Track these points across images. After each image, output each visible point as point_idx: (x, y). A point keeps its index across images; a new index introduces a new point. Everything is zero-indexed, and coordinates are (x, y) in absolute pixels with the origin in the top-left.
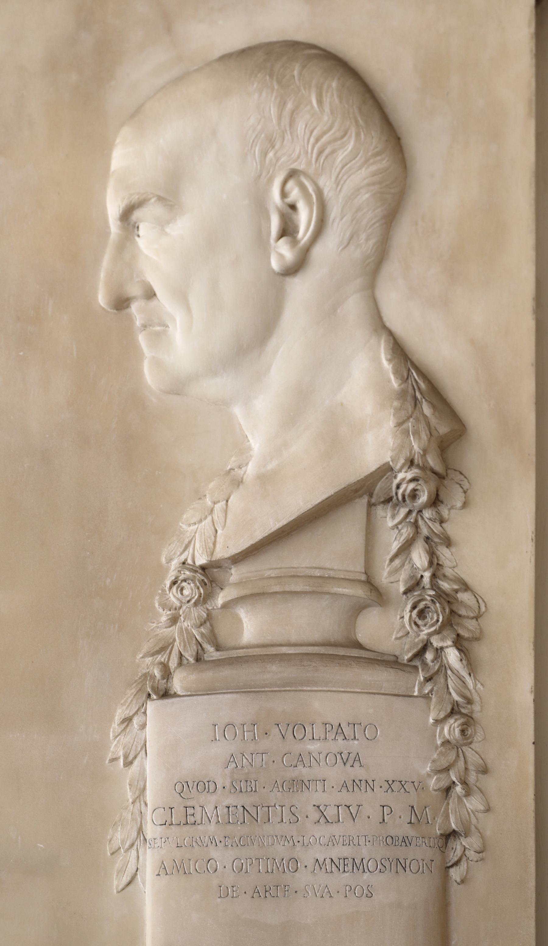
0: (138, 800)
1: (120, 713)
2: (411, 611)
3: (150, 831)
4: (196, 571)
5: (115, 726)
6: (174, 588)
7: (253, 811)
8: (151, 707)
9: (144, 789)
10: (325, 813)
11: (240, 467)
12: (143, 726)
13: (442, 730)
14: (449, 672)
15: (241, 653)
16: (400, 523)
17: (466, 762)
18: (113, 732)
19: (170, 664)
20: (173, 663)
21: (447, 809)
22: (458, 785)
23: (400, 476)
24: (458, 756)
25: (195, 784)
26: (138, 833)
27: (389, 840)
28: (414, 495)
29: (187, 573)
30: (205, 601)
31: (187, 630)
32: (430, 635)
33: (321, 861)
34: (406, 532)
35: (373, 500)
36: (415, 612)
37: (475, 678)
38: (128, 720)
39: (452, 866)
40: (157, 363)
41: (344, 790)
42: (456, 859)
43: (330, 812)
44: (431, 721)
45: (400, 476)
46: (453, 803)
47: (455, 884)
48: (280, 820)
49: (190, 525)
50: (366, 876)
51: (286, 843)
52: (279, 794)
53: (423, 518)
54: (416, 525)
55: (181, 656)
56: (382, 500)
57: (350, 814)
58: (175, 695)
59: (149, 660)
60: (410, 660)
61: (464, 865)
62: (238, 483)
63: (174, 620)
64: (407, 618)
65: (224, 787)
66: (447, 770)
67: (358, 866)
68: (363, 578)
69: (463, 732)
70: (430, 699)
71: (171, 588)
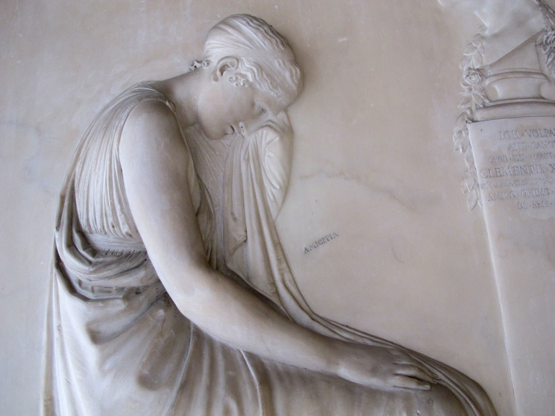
1: (456, 129)
6: (468, 78)
8: (470, 126)
12: (467, 134)
16: (548, 52)
18: (455, 138)
19: (472, 109)
20: (474, 108)
25: (498, 158)
31: (476, 94)
38: (460, 132)
48: (537, 172)
59: (463, 107)
63: (470, 90)
65: (510, 159)
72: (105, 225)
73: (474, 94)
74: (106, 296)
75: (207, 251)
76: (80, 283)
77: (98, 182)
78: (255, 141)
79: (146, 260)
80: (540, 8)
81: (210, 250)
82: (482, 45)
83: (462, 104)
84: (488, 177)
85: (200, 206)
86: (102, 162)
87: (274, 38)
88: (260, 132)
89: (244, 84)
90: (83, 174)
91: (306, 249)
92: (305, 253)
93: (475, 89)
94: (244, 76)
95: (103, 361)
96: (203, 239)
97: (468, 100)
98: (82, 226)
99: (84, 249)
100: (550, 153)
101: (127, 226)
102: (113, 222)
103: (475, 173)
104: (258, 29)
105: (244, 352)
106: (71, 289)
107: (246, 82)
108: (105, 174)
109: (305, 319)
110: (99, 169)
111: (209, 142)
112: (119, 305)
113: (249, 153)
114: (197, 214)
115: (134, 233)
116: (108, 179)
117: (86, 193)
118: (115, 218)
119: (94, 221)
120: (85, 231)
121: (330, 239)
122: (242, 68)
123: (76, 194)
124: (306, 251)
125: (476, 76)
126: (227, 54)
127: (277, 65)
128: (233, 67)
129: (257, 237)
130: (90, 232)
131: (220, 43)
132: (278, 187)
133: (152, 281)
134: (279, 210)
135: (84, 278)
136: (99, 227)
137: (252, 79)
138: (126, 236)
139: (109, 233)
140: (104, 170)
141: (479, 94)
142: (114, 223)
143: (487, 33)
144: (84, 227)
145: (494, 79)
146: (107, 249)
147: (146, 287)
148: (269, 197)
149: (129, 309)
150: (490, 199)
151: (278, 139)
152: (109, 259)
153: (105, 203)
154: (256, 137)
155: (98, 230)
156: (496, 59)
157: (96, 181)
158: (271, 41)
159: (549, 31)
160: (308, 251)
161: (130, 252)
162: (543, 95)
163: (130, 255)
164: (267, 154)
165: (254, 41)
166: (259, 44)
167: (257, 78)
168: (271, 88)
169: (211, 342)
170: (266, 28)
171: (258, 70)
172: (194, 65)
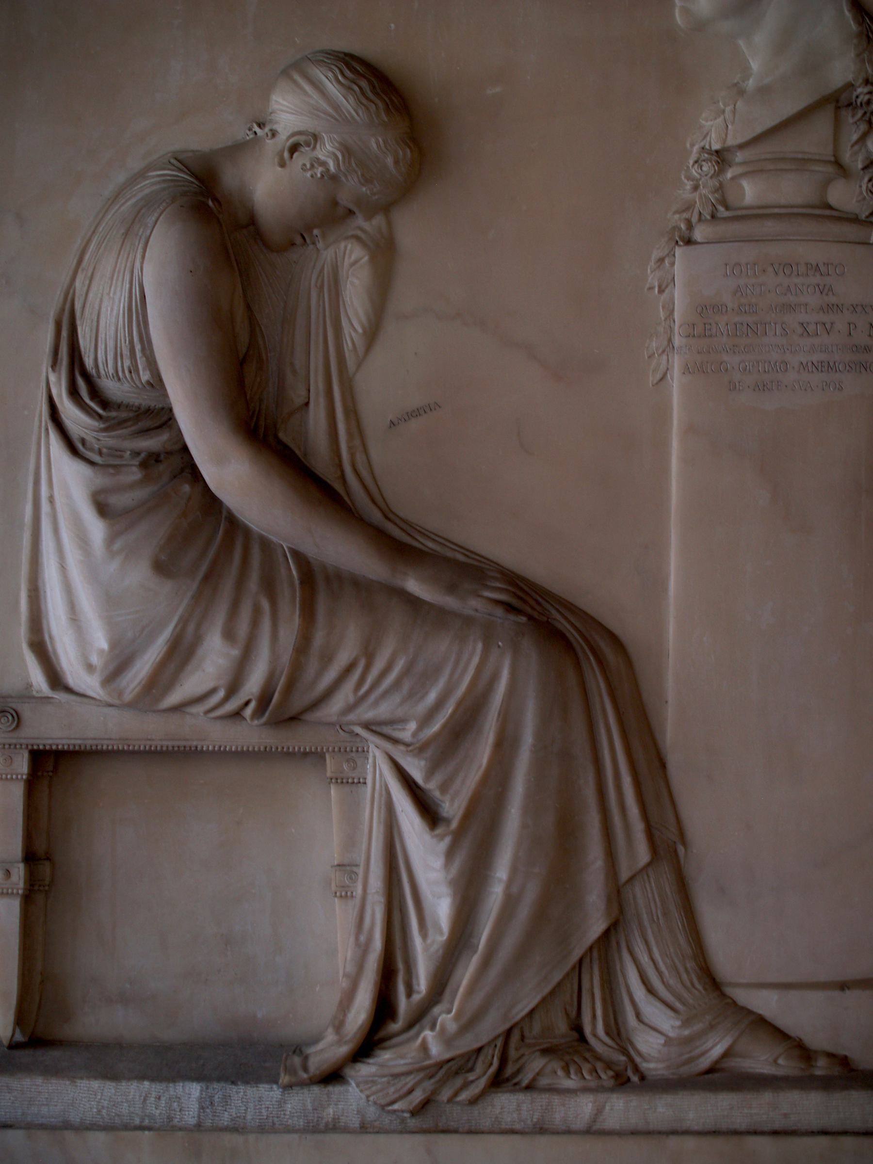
0: (668, 320)
1: (656, 255)
2: (868, 183)
3: (677, 341)
4: (712, 154)
5: (652, 263)
6: (696, 166)
8: (678, 251)
9: (673, 310)
11: (743, 82)
12: (673, 264)
15: (744, 212)
16: (858, 120)
18: (650, 269)
20: (694, 219)
26: (669, 344)
27: (854, 349)
29: (706, 155)
30: (718, 175)
31: (705, 195)
38: (661, 260)
40: (685, 11)
43: (811, 328)
45: (859, 90)
49: (707, 121)
51: (779, 350)
57: (825, 330)
58: (696, 243)
59: (677, 216)
60: (867, 217)
62: (741, 92)
63: (696, 188)
64: (864, 188)
67: (832, 367)
68: (832, 159)
71: (693, 165)
72: (120, 369)
74: (117, 462)
75: (254, 412)
76: (83, 442)
77: (112, 309)
78: (334, 259)
79: (170, 419)
80: (855, 41)
81: (257, 412)
83: (676, 212)
84: (689, 336)
85: (248, 351)
86: (119, 284)
87: (373, 103)
88: (342, 245)
89: (322, 176)
90: (91, 295)
91: (392, 423)
92: (390, 426)
93: (703, 187)
94: (323, 164)
95: (111, 540)
96: (248, 397)
97: (689, 207)
98: (87, 367)
99: (92, 399)
100: (806, 305)
101: (148, 372)
102: (131, 365)
103: (671, 329)
104: (350, 88)
105: (290, 549)
106: (72, 447)
107: (325, 174)
108: (122, 300)
109: (376, 516)
110: (115, 293)
111: (267, 255)
112: (134, 474)
113: (323, 276)
114: (242, 362)
115: (157, 383)
116: (126, 309)
117: (95, 324)
118: (133, 360)
119: (105, 362)
120: (90, 374)
121: (428, 410)
122: (322, 150)
123: (78, 322)
124: (392, 425)
126: (302, 127)
127: (374, 146)
128: (309, 146)
129: (322, 401)
130: (97, 376)
131: (293, 107)
132: (360, 330)
133: (177, 447)
134: (359, 365)
135: (90, 437)
136: (111, 370)
137: (335, 169)
138: (146, 386)
139: (124, 380)
140: (121, 295)
142: (132, 368)
143: (751, 84)
144: (91, 369)
146: (119, 401)
147: (169, 453)
148: (347, 343)
149: (146, 480)
150: (686, 370)
151: (366, 258)
152: (124, 415)
153: (121, 340)
154: (336, 253)
155: (109, 374)
156: (749, 136)
157: (109, 309)
158: (368, 109)
159: (859, 87)
160: (394, 425)
161: (149, 407)
163: (150, 411)
164: (350, 279)
165: (342, 108)
166: (350, 113)
167: (342, 168)
168: (362, 181)
169: (247, 532)
170: (364, 84)
171: (343, 156)
172: (254, 130)
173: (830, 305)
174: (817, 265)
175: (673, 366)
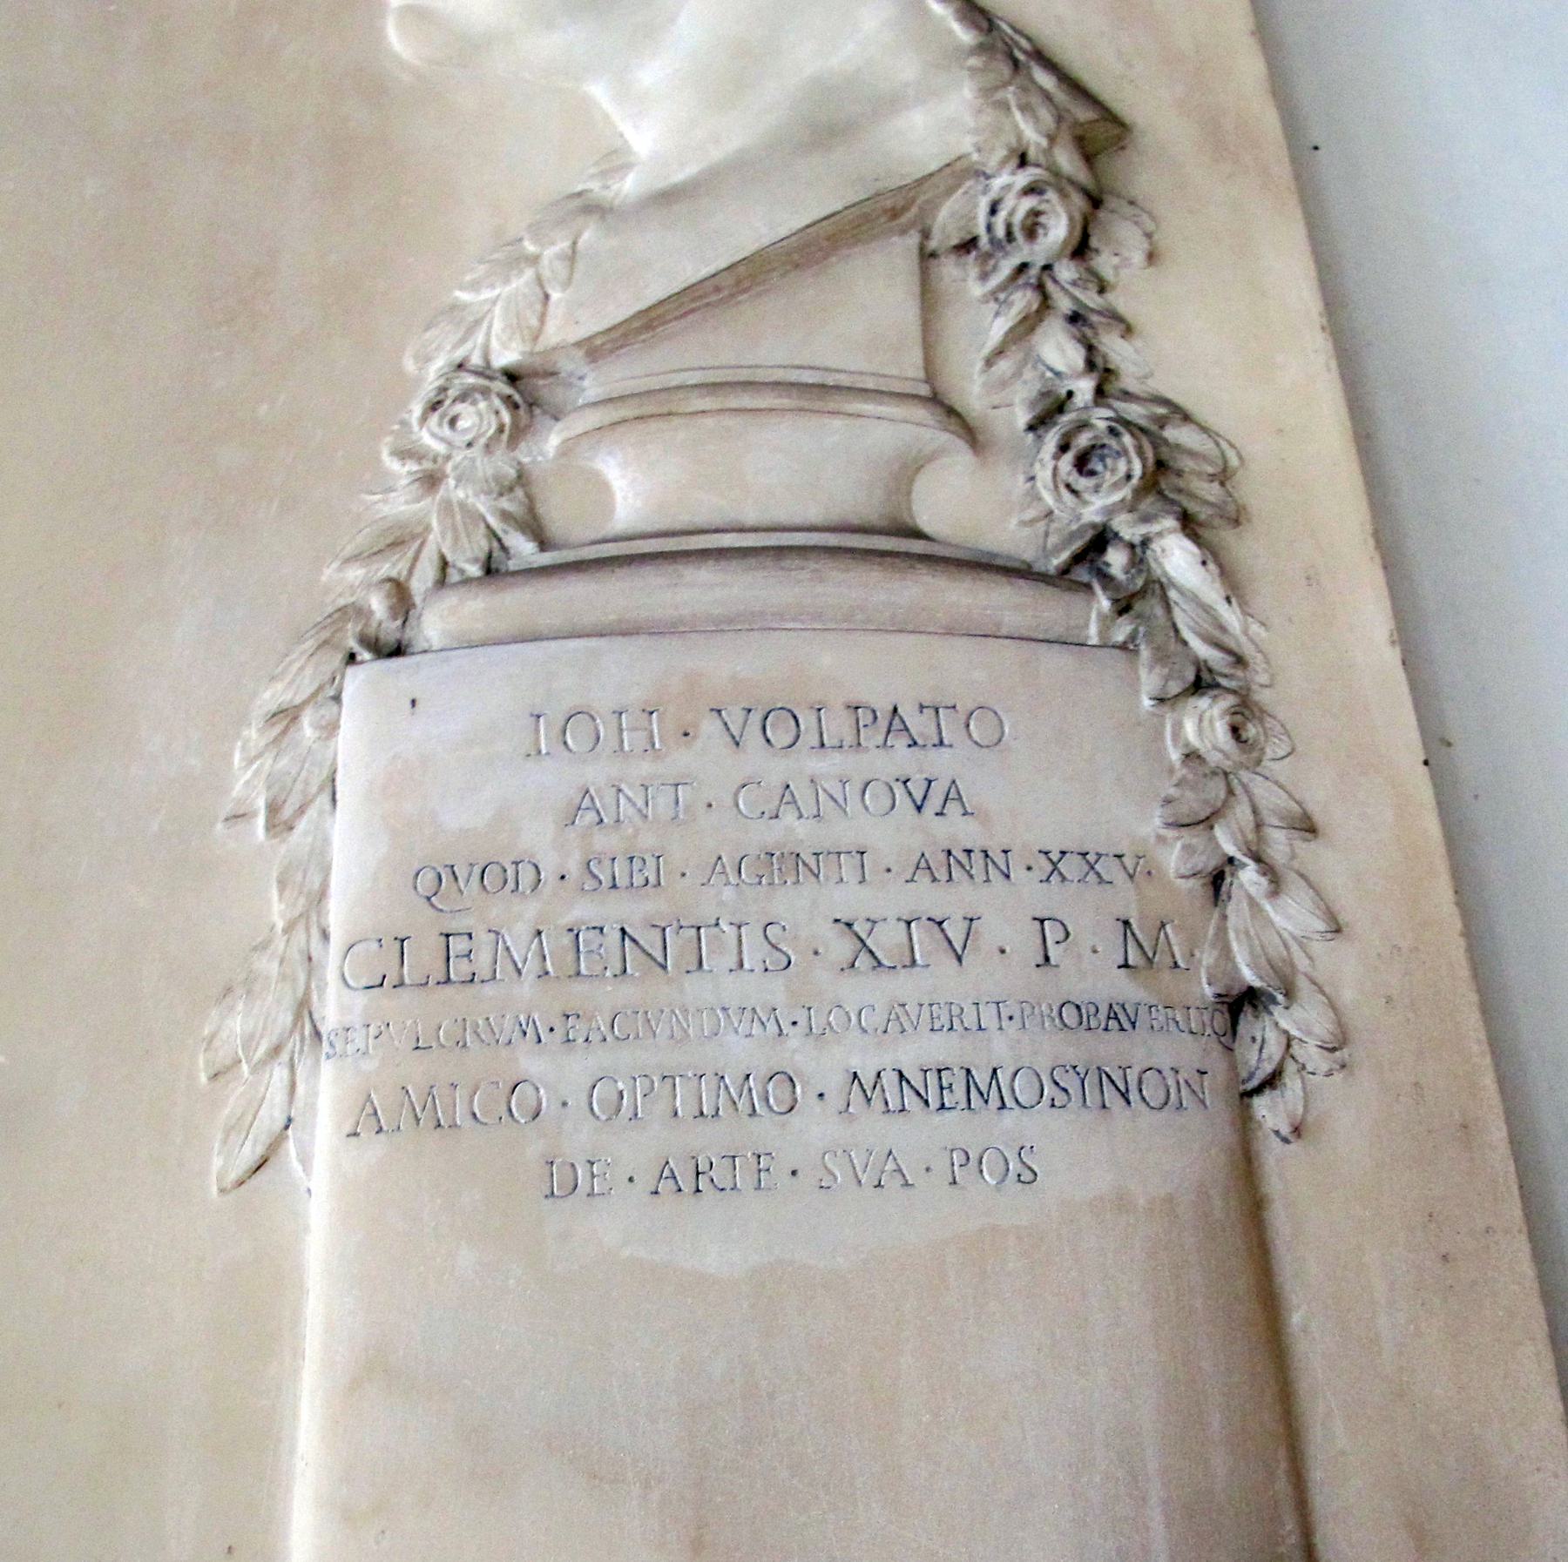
0: (301, 927)
2: (1056, 457)
3: (332, 1009)
4: (490, 378)
6: (434, 418)
7: (650, 940)
9: (323, 894)
10: (869, 942)
12: (331, 728)
13: (1178, 727)
14: (1173, 594)
16: (1003, 287)
17: (1255, 811)
18: (243, 748)
21: (1222, 931)
22: (1244, 865)
23: (997, 183)
24: (1231, 792)
25: (477, 870)
26: (298, 1017)
27: (1069, 1015)
28: (1032, 229)
29: (471, 380)
30: (514, 441)
32: (1111, 511)
33: (867, 1079)
34: (1023, 300)
35: (933, 244)
36: (1069, 457)
37: (1245, 613)
38: (288, 716)
39: (1258, 1090)
41: (923, 879)
42: (1268, 1068)
43: (887, 940)
44: (1147, 703)
46: (1236, 911)
47: (1275, 1142)
48: (732, 961)
50: (1010, 1118)
51: (756, 1029)
52: (728, 894)
53: (1055, 281)
54: (1040, 287)
55: (444, 564)
56: (955, 241)
57: (946, 944)
59: (355, 573)
61: (1292, 1083)
63: (431, 481)
64: (1044, 475)
65: (563, 877)
66: (1207, 822)
67: (984, 1089)
69: (1235, 731)
70: (1136, 652)
71: (424, 419)
73: (447, 507)
82: (575, 243)
93: (459, 480)
97: (400, 539)
125: (482, 405)
141: (482, 505)
143: (629, 186)
145: (593, 419)
162: (925, 522)
173: (957, 853)
174: (895, 710)
175: (312, 1107)
